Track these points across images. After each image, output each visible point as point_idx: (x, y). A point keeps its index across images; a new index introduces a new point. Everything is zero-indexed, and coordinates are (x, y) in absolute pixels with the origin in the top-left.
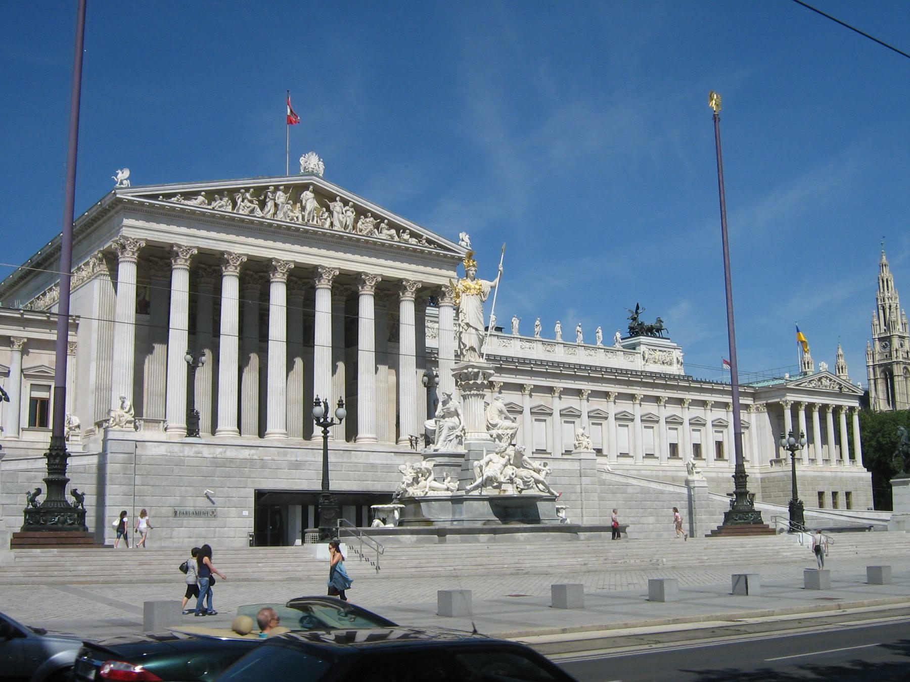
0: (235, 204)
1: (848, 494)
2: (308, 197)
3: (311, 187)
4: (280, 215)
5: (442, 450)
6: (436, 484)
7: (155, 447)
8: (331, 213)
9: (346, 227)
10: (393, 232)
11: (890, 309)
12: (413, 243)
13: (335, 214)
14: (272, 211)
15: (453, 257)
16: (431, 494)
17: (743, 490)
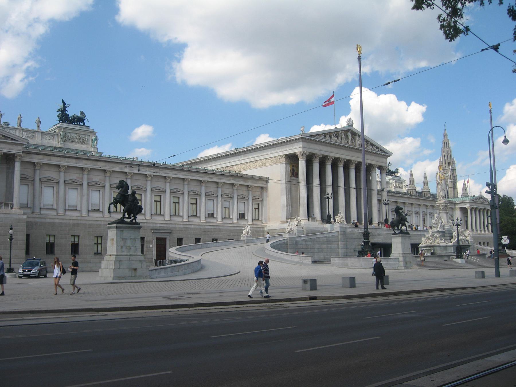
0: (330, 137)
1: (488, 243)
2: (349, 134)
3: (350, 131)
4: (343, 142)
5: (440, 230)
6: (441, 241)
7: (349, 229)
8: (355, 140)
9: (359, 145)
10: (371, 147)
11: (448, 156)
12: (377, 151)
13: (357, 141)
14: (340, 141)
15: (387, 156)
16: (441, 244)
17: (500, 243)
